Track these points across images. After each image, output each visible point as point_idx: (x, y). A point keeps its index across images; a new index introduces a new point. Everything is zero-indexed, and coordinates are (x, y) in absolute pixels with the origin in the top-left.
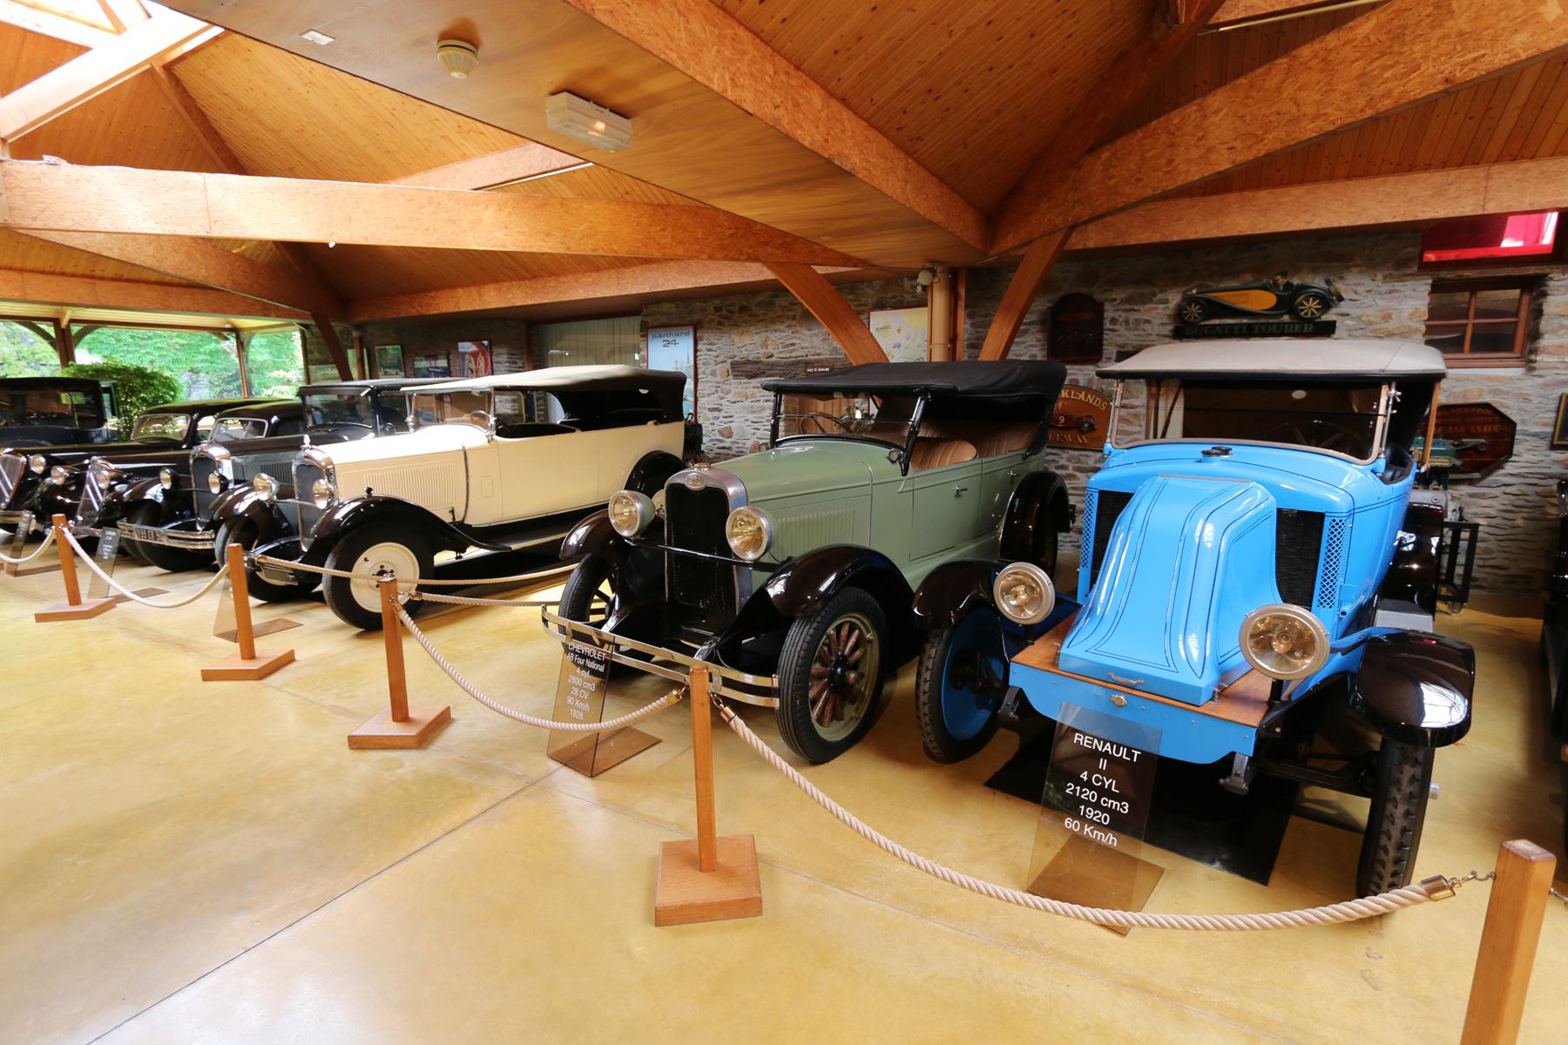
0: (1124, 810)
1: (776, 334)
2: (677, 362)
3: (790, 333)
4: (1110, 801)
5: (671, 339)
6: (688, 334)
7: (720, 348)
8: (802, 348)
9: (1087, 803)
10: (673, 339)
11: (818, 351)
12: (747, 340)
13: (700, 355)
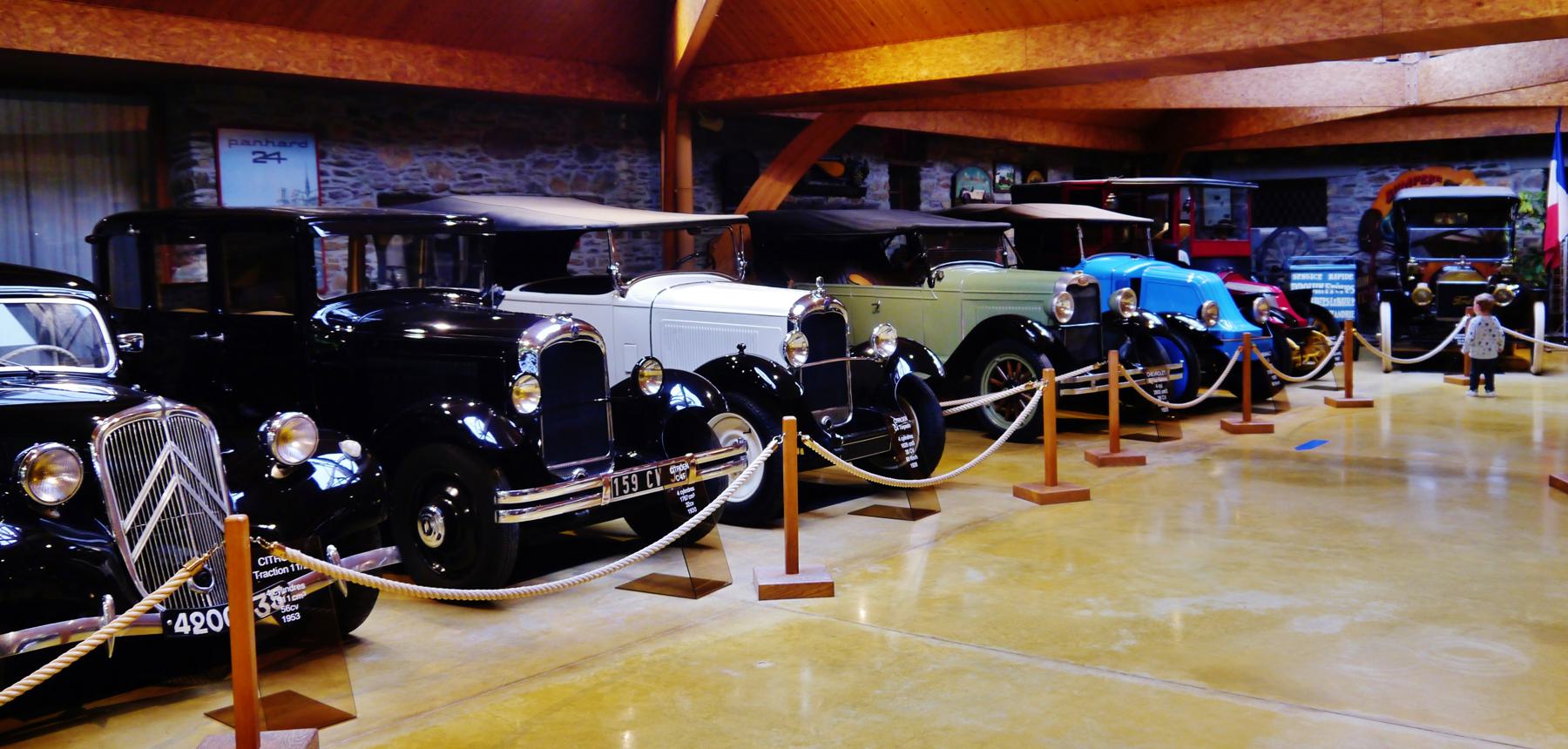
1: (454, 160)
2: (284, 191)
3: (473, 160)
5: (269, 150)
6: (303, 145)
7: (361, 173)
8: (490, 181)
10: (277, 149)
11: (511, 187)
12: (405, 165)
13: (327, 182)
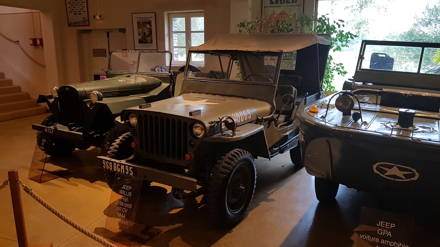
0: (130, 207)
4: (127, 204)
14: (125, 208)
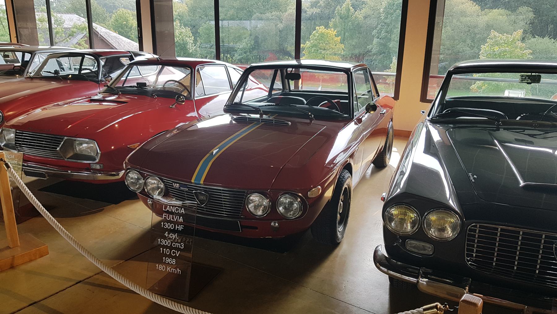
0: (182, 247)
4: (176, 244)
9: (166, 256)
14: (175, 249)
